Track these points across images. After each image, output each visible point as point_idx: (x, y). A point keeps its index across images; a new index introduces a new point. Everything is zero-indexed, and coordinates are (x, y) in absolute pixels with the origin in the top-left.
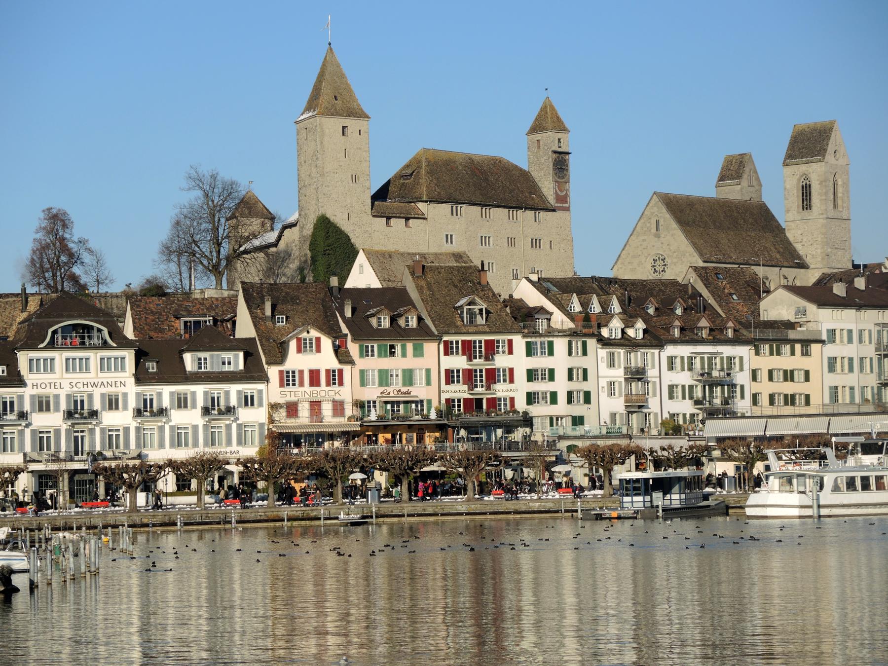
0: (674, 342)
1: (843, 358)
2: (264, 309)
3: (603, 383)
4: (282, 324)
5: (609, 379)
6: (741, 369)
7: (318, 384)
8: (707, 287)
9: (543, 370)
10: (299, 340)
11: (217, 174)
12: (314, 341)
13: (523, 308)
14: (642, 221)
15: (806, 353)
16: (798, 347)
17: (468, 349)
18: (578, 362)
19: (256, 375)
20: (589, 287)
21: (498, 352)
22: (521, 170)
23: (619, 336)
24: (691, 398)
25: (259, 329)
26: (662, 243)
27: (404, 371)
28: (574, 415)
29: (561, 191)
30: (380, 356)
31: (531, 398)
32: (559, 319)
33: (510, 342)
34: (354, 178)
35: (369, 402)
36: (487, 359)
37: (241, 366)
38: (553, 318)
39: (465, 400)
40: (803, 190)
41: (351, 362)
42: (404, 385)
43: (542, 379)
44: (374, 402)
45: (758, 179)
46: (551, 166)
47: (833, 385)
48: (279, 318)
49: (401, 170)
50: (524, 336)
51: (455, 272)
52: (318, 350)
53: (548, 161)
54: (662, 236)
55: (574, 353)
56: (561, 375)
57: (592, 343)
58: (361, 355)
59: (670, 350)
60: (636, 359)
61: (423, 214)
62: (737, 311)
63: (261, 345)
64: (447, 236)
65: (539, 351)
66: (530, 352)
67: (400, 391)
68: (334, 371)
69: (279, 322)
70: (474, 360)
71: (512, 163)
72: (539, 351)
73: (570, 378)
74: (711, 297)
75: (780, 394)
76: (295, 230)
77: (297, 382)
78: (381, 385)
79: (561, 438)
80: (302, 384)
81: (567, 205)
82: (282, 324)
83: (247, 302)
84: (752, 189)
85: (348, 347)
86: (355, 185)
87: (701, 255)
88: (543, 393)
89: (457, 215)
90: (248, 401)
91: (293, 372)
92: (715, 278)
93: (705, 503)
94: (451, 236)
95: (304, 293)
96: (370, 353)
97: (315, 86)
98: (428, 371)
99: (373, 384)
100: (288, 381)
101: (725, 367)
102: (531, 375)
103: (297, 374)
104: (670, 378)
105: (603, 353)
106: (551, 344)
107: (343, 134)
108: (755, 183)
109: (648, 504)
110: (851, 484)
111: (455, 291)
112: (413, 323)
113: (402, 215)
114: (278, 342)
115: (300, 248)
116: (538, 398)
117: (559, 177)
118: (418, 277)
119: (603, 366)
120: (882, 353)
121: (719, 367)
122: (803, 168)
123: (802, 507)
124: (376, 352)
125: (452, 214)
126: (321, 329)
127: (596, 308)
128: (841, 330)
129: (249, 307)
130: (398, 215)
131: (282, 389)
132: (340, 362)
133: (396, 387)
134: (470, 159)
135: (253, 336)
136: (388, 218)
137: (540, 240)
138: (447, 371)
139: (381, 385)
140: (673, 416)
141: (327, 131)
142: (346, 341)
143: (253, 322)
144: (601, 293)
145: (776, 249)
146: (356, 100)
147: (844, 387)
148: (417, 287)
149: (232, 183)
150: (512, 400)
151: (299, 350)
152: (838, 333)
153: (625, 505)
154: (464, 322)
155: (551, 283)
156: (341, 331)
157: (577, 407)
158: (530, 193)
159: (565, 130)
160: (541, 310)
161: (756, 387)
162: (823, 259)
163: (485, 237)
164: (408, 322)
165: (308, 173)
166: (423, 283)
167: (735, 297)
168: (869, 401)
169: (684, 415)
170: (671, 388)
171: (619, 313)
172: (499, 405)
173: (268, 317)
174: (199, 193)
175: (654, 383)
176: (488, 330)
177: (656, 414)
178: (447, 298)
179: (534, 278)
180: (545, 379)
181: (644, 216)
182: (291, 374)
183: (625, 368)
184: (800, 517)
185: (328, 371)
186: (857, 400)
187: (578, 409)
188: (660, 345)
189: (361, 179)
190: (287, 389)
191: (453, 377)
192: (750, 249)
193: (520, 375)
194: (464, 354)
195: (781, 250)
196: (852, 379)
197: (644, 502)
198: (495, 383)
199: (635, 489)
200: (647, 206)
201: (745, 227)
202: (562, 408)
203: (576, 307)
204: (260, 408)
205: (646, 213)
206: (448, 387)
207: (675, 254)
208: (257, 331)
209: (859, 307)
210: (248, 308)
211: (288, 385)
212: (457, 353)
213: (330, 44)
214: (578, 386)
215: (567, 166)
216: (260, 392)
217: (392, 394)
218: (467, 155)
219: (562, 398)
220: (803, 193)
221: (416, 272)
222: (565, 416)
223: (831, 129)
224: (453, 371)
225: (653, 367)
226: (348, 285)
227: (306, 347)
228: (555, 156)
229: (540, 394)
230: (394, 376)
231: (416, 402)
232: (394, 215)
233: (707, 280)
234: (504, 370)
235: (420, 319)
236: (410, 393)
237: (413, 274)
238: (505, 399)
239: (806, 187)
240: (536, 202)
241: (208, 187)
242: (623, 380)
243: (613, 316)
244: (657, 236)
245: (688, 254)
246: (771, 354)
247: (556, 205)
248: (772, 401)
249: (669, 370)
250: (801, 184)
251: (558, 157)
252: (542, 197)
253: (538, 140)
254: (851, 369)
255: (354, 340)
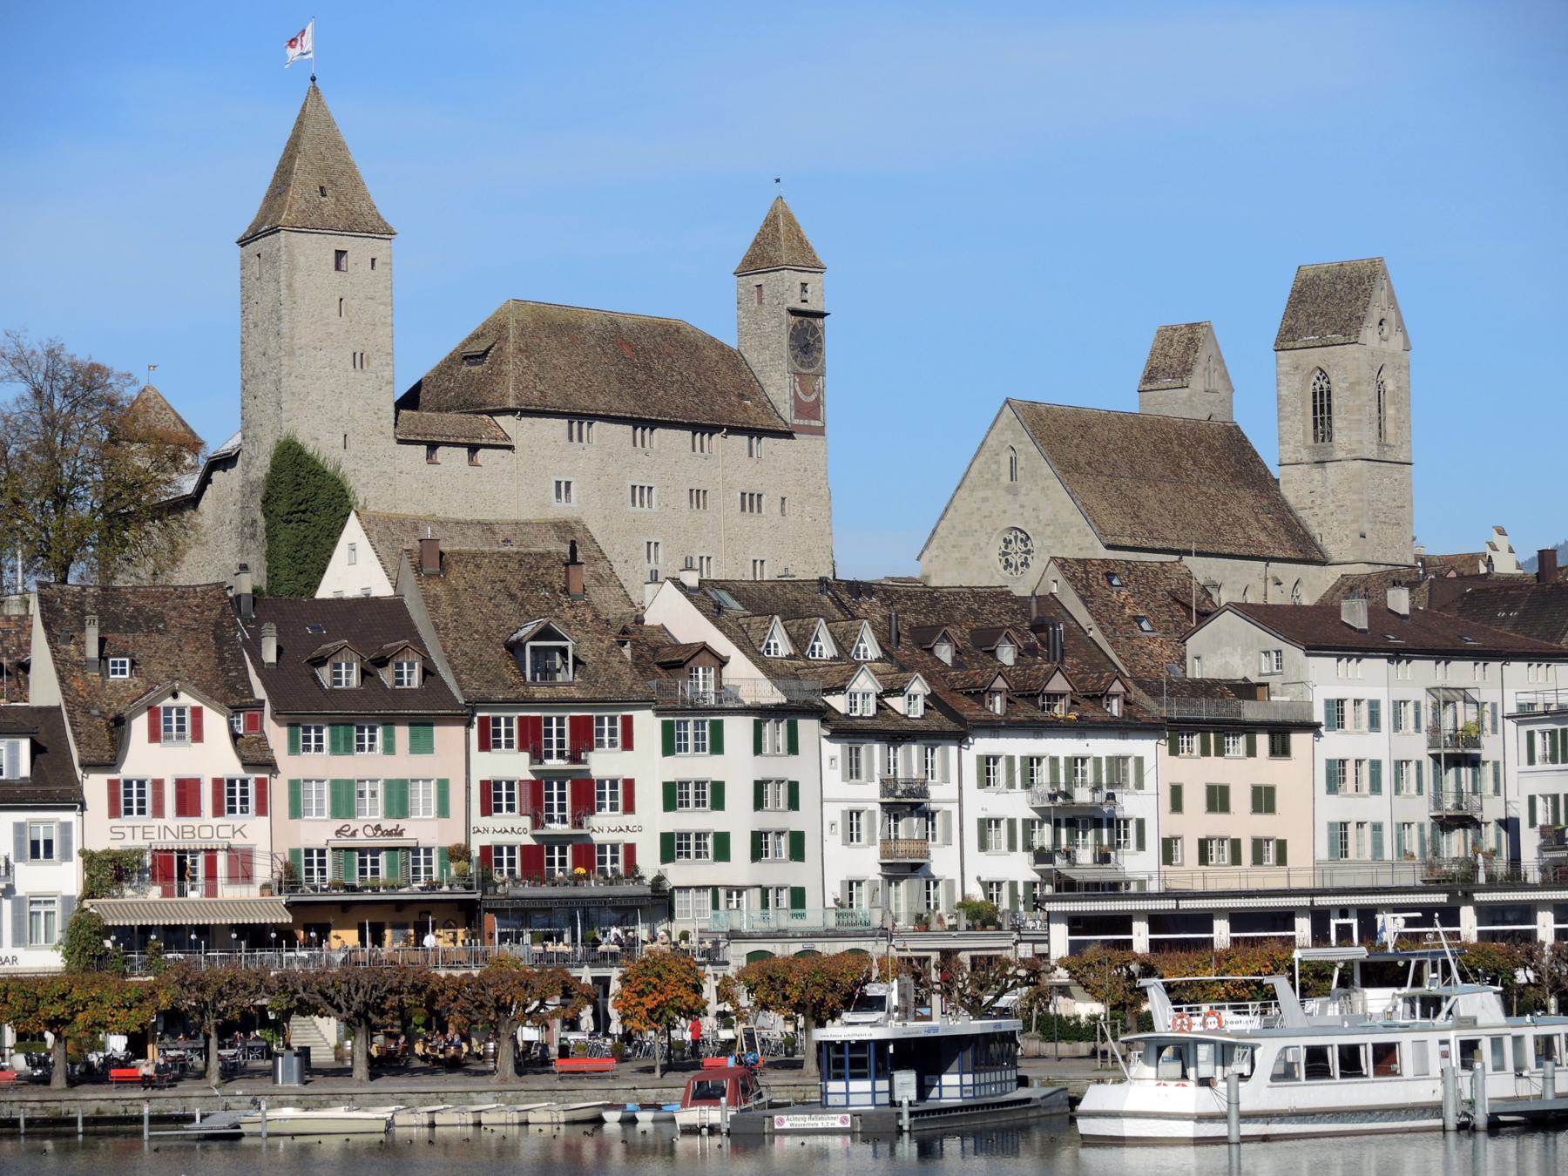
0: (994, 728)
1: (1359, 762)
2: (83, 643)
3: (834, 813)
4: (121, 677)
5: (847, 807)
6: (1140, 785)
7: (196, 812)
8: (1085, 603)
9: (700, 784)
10: (153, 712)
11: (61, 347)
12: (188, 716)
13: (664, 646)
14: (981, 459)
15: (1280, 749)
16: (1263, 740)
17: (533, 739)
18: (778, 766)
19: (57, 789)
20: (813, 601)
21: (601, 744)
22: (722, 347)
23: (872, 711)
24: (1028, 847)
25: (69, 687)
26: (1022, 506)
27: (389, 784)
28: (765, 884)
29: (807, 394)
30: (335, 749)
31: (671, 846)
32: (741, 670)
33: (628, 722)
34: (359, 360)
35: (309, 852)
36: (575, 758)
37: (25, 770)
38: (727, 671)
39: (525, 848)
40: (1315, 402)
41: (271, 766)
42: (389, 814)
43: (697, 804)
44: (322, 852)
45: (1225, 376)
46: (785, 340)
47: (1338, 819)
48: (114, 664)
49: (464, 345)
50: (659, 712)
51: (513, 566)
52: (198, 736)
53: (779, 330)
54: (1023, 490)
55: (767, 748)
56: (739, 796)
57: (809, 729)
58: (293, 749)
59: (983, 745)
60: (909, 759)
61: (507, 438)
62: (1150, 656)
63: (72, 724)
64: (558, 483)
65: (691, 742)
66: (670, 745)
67: (378, 827)
68: (231, 782)
69: (115, 672)
70: (548, 762)
71: (702, 333)
72: (691, 742)
73: (759, 803)
74: (1094, 626)
75: (1222, 840)
76: (235, 472)
77: (149, 806)
78: (336, 814)
79: (734, 935)
80: (159, 811)
81: (818, 423)
82: (121, 677)
83: (47, 626)
84: (1212, 397)
85: (265, 729)
86: (360, 375)
87: (1102, 533)
88: (698, 836)
89: (580, 440)
90: (39, 850)
91: (141, 783)
92: (1104, 583)
93: (1022, 1093)
94: (568, 484)
95: (175, 609)
96: (313, 744)
97: (280, 166)
98: (443, 785)
99: (320, 812)
100: (128, 803)
101: (1104, 781)
102: (673, 796)
103: (148, 789)
104: (982, 804)
105: (834, 750)
106: (717, 729)
107: (338, 267)
108: (1217, 383)
109: (884, 1099)
110: (1317, 1063)
111: (509, 607)
112: (414, 680)
113: (461, 440)
114: (111, 715)
115: (243, 508)
116: (688, 846)
117: (802, 365)
118: (429, 576)
119: (834, 779)
120: (1443, 751)
121: (1090, 778)
122: (1315, 357)
123: (1200, 1118)
124: (326, 743)
125: (571, 439)
126: (207, 691)
127: (825, 647)
128: (1357, 702)
129: (52, 638)
130: (452, 440)
131: (115, 821)
132: (247, 765)
133: (371, 816)
134: (612, 322)
135: (55, 703)
136: (432, 446)
137: (760, 496)
138: (485, 785)
139: (336, 814)
140: (987, 886)
141: (302, 259)
142: (262, 716)
143: (58, 671)
144: (839, 615)
145: (1258, 520)
146: (365, 197)
147: (1360, 825)
148: (426, 597)
149: (95, 368)
150: (630, 849)
151: (154, 736)
152: (1348, 706)
153: (831, 1100)
154: (525, 677)
155: (729, 590)
156: (251, 694)
157: (776, 866)
158: (741, 396)
159: (817, 268)
160: (704, 648)
161: (1174, 825)
162: (1353, 544)
163: (642, 488)
164: (401, 674)
165: (261, 349)
166: (438, 589)
167: (1145, 625)
168: (1412, 856)
169: (1013, 885)
170: (985, 825)
171: (878, 660)
172: (603, 861)
173: (92, 661)
174: (23, 389)
175: (948, 814)
176: (578, 695)
177: (950, 883)
178: (493, 623)
179: (691, 579)
180: (704, 804)
181: (985, 448)
182: (135, 789)
183: (882, 782)
184: (1199, 1141)
185: (217, 783)
186: (1389, 853)
187: (779, 871)
188: (960, 738)
189: (374, 363)
190: (125, 821)
191: (498, 798)
192: (1205, 521)
193: (649, 797)
194: (523, 747)
195: (1270, 523)
196: (1377, 808)
197: (874, 1092)
198: (592, 813)
199: (855, 1063)
200: (992, 428)
201: (1195, 475)
202: (739, 868)
203: (781, 644)
204: (66, 864)
205: (989, 442)
206: (487, 821)
207: (1050, 529)
208: (64, 693)
209: (1397, 655)
210: (49, 641)
211: (129, 812)
212: (509, 745)
213: (313, 79)
214: (772, 819)
215: (819, 340)
216: (66, 827)
217: (360, 835)
218: (605, 313)
219: (740, 847)
220: (1315, 407)
221: (424, 564)
222: (746, 888)
223: (1372, 277)
224: (498, 785)
225: (946, 779)
226: (325, 591)
227: (170, 729)
228: (793, 319)
229: (692, 837)
230: (367, 794)
231: (416, 850)
232: (444, 439)
233: (1088, 587)
234: (614, 784)
235: (428, 672)
236: (401, 833)
237: (418, 568)
238: (614, 849)
239: (1322, 393)
240: (753, 414)
241: (41, 377)
242: (877, 808)
243: (858, 664)
244: (1013, 491)
245: (1074, 530)
246: (1205, 752)
247: (796, 422)
248: (1204, 858)
249: (980, 786)
250: (1312, 387)
251: (800, 322)
252: (768, 407)
253: (759, 286)
254: (1376, 787)
255: (277, 715)
